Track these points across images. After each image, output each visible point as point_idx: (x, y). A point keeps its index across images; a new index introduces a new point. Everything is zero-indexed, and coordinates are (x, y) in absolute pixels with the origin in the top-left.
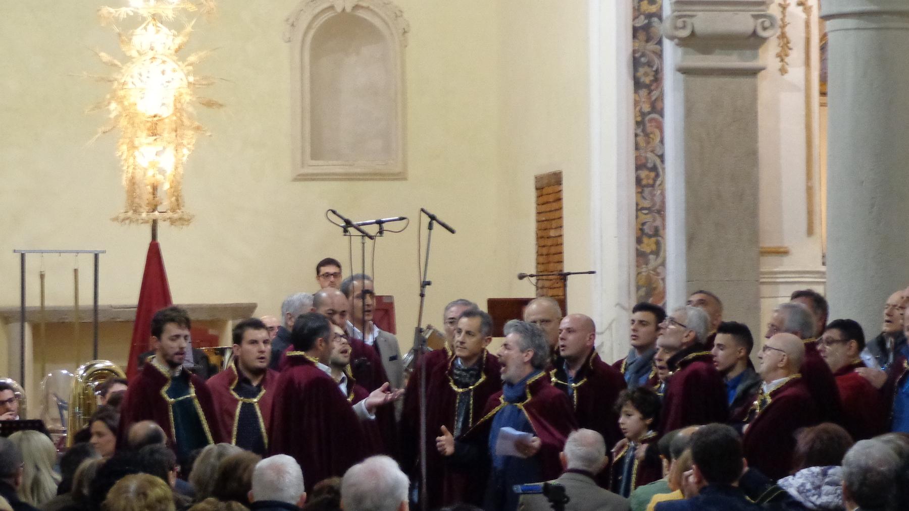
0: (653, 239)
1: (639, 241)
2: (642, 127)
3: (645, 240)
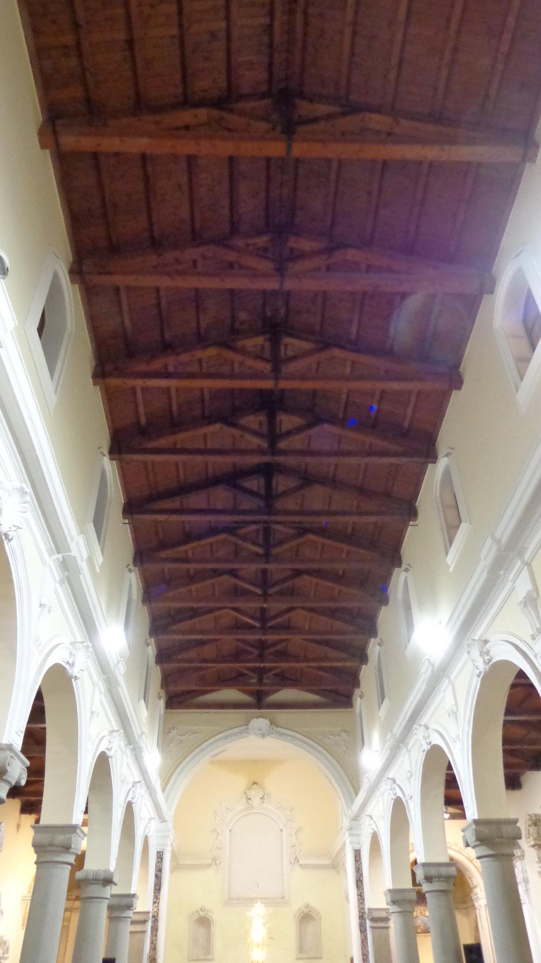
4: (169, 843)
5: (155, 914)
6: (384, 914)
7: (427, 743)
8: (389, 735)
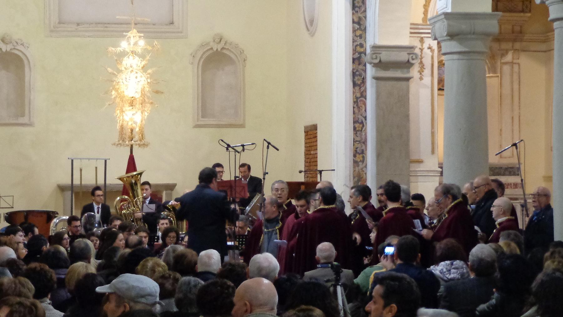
0: (361, 155)
1: (355, 156)
2: (356, 104)
3: (358, 155)
6: (403, 57)
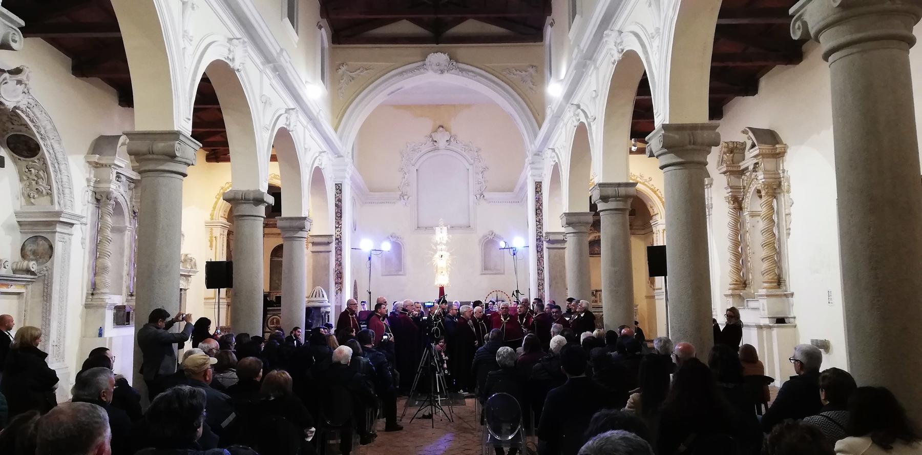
1: (539, 286)
4: (348, 176)
5: (338, 237)
6: (561, 237)
7: (618, 52)
8: (576, 50)
